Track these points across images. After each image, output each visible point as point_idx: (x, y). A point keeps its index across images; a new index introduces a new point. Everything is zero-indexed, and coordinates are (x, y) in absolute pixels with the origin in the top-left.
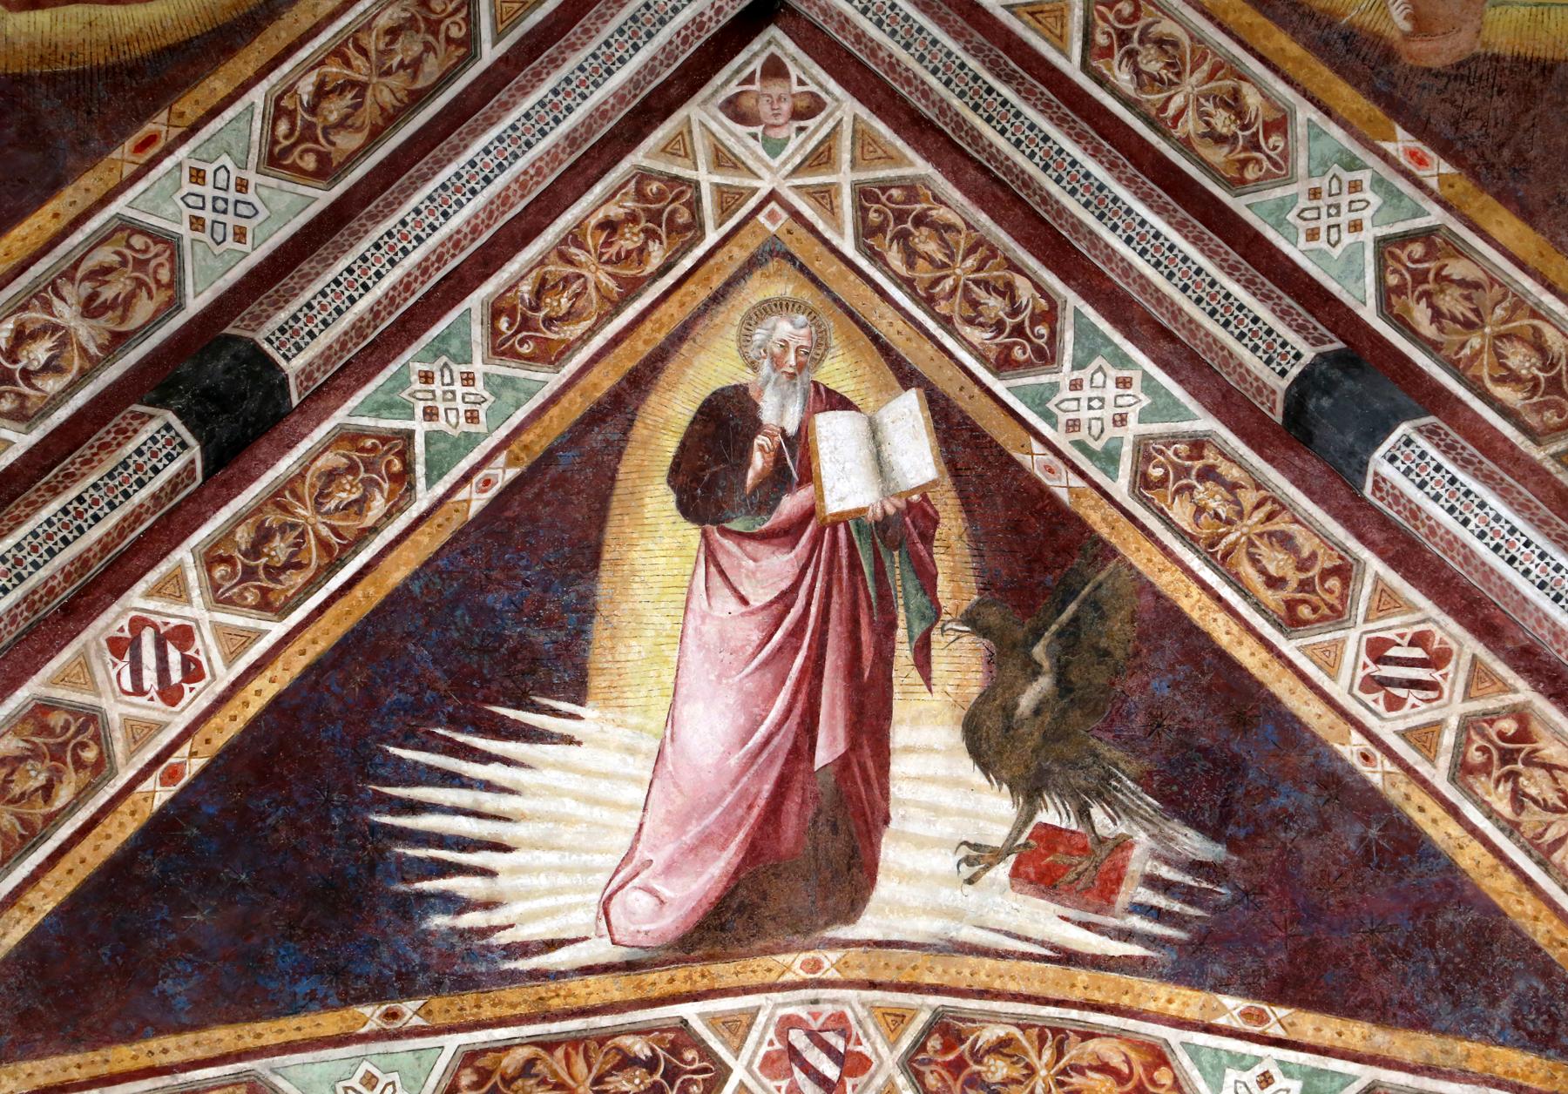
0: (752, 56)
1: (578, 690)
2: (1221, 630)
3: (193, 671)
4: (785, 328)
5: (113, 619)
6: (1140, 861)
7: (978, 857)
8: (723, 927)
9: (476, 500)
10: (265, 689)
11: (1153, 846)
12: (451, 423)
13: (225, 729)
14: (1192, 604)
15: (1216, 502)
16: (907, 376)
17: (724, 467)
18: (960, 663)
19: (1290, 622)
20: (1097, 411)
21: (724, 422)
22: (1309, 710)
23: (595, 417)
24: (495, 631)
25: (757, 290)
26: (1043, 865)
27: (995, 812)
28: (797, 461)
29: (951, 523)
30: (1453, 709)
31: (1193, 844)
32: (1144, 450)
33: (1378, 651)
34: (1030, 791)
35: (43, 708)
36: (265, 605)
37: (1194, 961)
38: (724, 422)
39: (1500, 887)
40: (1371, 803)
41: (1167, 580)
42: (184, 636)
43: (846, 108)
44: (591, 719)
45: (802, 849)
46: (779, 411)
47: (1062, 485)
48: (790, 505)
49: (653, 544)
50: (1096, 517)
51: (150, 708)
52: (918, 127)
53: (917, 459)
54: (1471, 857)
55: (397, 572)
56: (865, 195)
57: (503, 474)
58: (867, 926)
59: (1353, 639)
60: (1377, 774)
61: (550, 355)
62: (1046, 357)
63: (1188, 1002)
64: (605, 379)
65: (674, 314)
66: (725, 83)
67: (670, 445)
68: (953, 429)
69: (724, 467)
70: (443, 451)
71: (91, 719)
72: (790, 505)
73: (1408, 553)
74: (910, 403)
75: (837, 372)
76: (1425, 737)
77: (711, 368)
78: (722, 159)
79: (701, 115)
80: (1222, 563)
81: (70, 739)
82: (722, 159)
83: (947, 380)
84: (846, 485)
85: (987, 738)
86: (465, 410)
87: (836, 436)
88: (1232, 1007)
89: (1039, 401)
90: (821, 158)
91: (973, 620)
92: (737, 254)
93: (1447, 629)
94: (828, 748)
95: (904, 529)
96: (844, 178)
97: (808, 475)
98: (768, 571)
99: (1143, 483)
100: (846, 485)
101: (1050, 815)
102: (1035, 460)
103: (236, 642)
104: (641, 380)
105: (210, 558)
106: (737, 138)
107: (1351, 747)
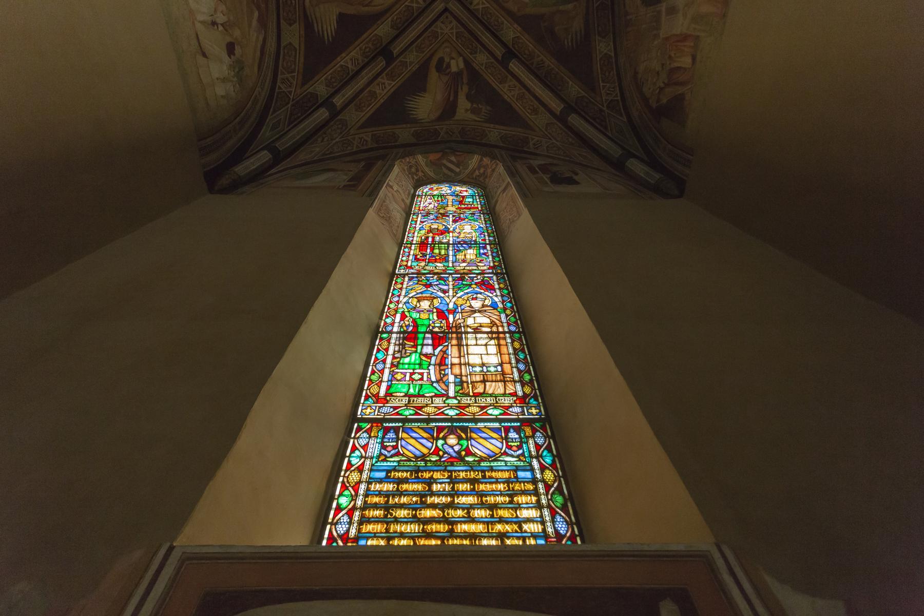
0: (444, 16)
1: (425, 90)
4: (448, 50)
5: (376, 82)
7: (467, 110)
8: (440, 118)
10: (392, 90)
13: (389, 94)
16: (461, 55)
17: (441, 67)
18: (465, 89)
19: (500, 83)
20: (481, 59)
21: (441, 60)
22: (501, 93)
24: (417, 83)
26: (473, 111)
27: (468, 105)
28: (449, 66)
29: (465, 72)
31: (488, 108)
35: (370, 91)
36: (393, 81)
38: (441, 60)
41: (488, 79)
43: (454, 22)
45: (449, 110)
46: (447, 60)
47: (477, 68)
48: (448, 71)
49: (433, 75)
52: (463, 25)
53: (462, 65)
55: (407, 76)
56: (457, 33)
57: (417, 66)
58: (456, 118)
60: (508, 100)
62: (476, 53)
63: (487, 125)
66: (441, 19)
68: (466, 61)
69: (441, 67)
70: (411, 63)
71: (375, 92)
73: (513, 75)
74: (461, 58)
76: (513, 96)
78: (441, 29)
79: (438, 23)
82: (441, 29)
84: (454, 69)
85: (469, 97)
86: (413, 59)
87: (453, 63)
88: (492, 125)
89: (475, 58)
90: (452, 28)
93: (517, 83)
95: (459, 74)
96: (454, 31)
100: (454, 69)
102: (474, 65)
105: (387, 75)
106: (442, 25)
107: (506, 97)
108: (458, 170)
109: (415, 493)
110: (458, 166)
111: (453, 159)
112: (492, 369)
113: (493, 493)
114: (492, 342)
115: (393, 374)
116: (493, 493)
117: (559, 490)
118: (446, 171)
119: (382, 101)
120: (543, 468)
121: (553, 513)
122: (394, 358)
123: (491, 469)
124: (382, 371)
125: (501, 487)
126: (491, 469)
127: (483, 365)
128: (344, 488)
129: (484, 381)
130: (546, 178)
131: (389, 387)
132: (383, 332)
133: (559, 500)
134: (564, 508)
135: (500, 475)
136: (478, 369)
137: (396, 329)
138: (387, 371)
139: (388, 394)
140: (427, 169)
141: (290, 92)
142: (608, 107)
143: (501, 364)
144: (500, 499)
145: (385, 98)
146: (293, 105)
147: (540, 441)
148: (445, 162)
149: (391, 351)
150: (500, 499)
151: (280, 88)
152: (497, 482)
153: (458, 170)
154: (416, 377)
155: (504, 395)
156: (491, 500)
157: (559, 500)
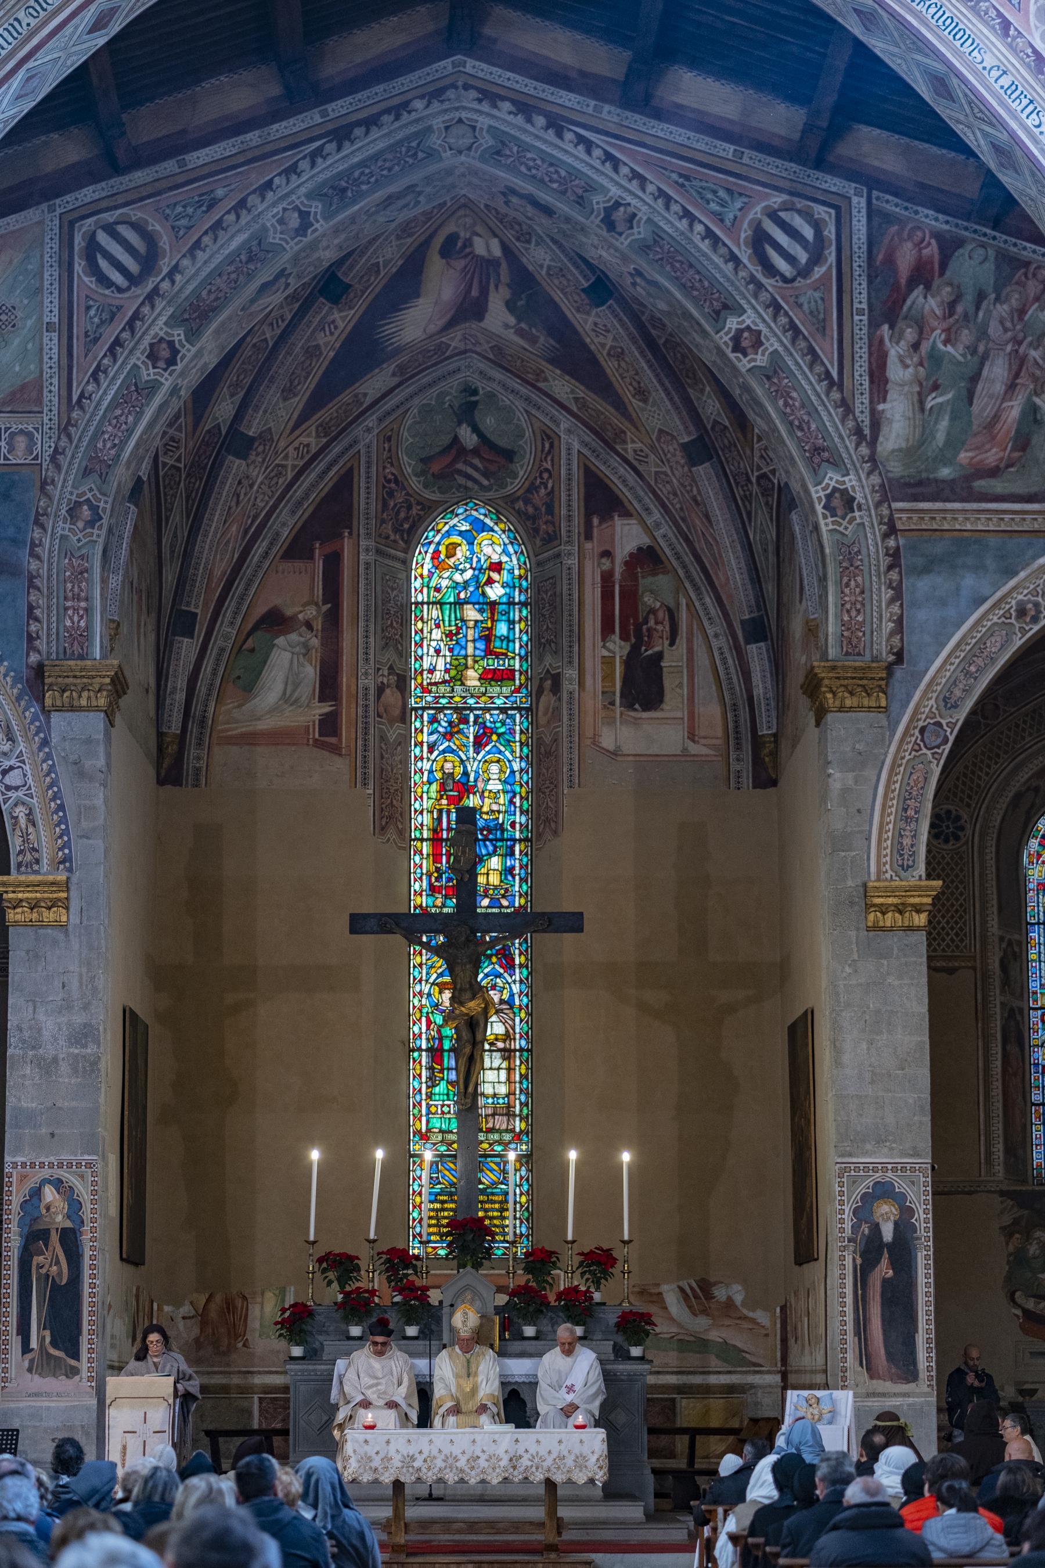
1: (418, 296)
2: (564, 309)
3: (336, 328)
6: (542, 339)
7: (507, 326)
9: (394, 270)
11: (543, 339)
12: (389, 256)
13: (344, 336)
14: (557, 299)
15: (565, 282)
16: (495, 235)
18: (505, 292)
21: (452, 239)
23: (421, 245)
25: (461, 212)
26: (520, 333)
27: (512, 321)
28: (468, 243)
29: (504, 266)
30: (609, 343)
32: (549, 268)
33: (596, 324)
34: (519, 320)
37: (551, 361)
39: (613, 379)
40: (590, 351)
41: (552, 293)
42: (333, 322)
44: (421, 300)
45: (469, 310)
47: (530, 268)
48: (468, 250)
49: (435, 264)
50: (538, 277)
51: (329, 338)
53: (497, 252)
54: (608, 371)
57: (400, 263)
58: (482, 324)
59: (591, 320)
61: (410, 235)
62: (529, 242)
64: (423, 238)
65: (439, 221)
67: (439, 246)
68: (505, 248)
70: (386, 263)
71: (318, 347)
72: (468, 250)
75: (479, 229)
76: (603, 345)
77: (450, 228)
80: (565, 294)
81: (312, 352)
83: (505, 239)
84: (479, 247)
85: (510, 306)
87: (477, 240)
89: (527, 249)
91: (508, 285)
92: (456, 206)
94: (475, 293)
95: (492, 263)
97: (471, 245)
98: (460, 264)
99: (548, 274)
100: (479, 247)
101: (523, 325)
102: (524, 260)
103: (343, 318)
104: (431, 237)
107: (588, 340)
108: (486, 482)
109: (451, 1210)
110: (486, 475)
111: (476, 461)
112: (501, 1101)
113: (493, 1210)
114: (504, 1065)
115: (428, 1106)
116: (493, 1210)
117: (527, 1209)
118: (461, 480)
119: (332, 354)
120: (521, 1194)
121: (521, 1222)
122: (428, 1087)
123: (493, 1194)
124: (420, 1104)
125: (497, 1206)
126: (493, 1194)
127: (495, 1095)
128: (414, 1207)
129: (493, 1115)
130: (618, 648)
131: (428, 1122)
132: (413, 1050)
133: (526, 1214)
134: (527, 1220)
135: (496, 1198)
136: (490, 1101)
137: (424, 1047)
138: (424, 1103)
139: (428, 1130)
140: (428, 495)
141: (179, 460)
142: (759, 478)
143: (508, 1096)
144: (495, 1214)
145: (337, 345)
146: (188, 475)
147: (523, 1173)
148: (460, 466)
149: (424, 1079)
150: (495, 1214)
151: (165, 464)
152: (495, 1202)
153: (486, 482)
154: (446, 1109)
155: (507, 1131)
156: (490, 1214)
157: (526, 1214)
